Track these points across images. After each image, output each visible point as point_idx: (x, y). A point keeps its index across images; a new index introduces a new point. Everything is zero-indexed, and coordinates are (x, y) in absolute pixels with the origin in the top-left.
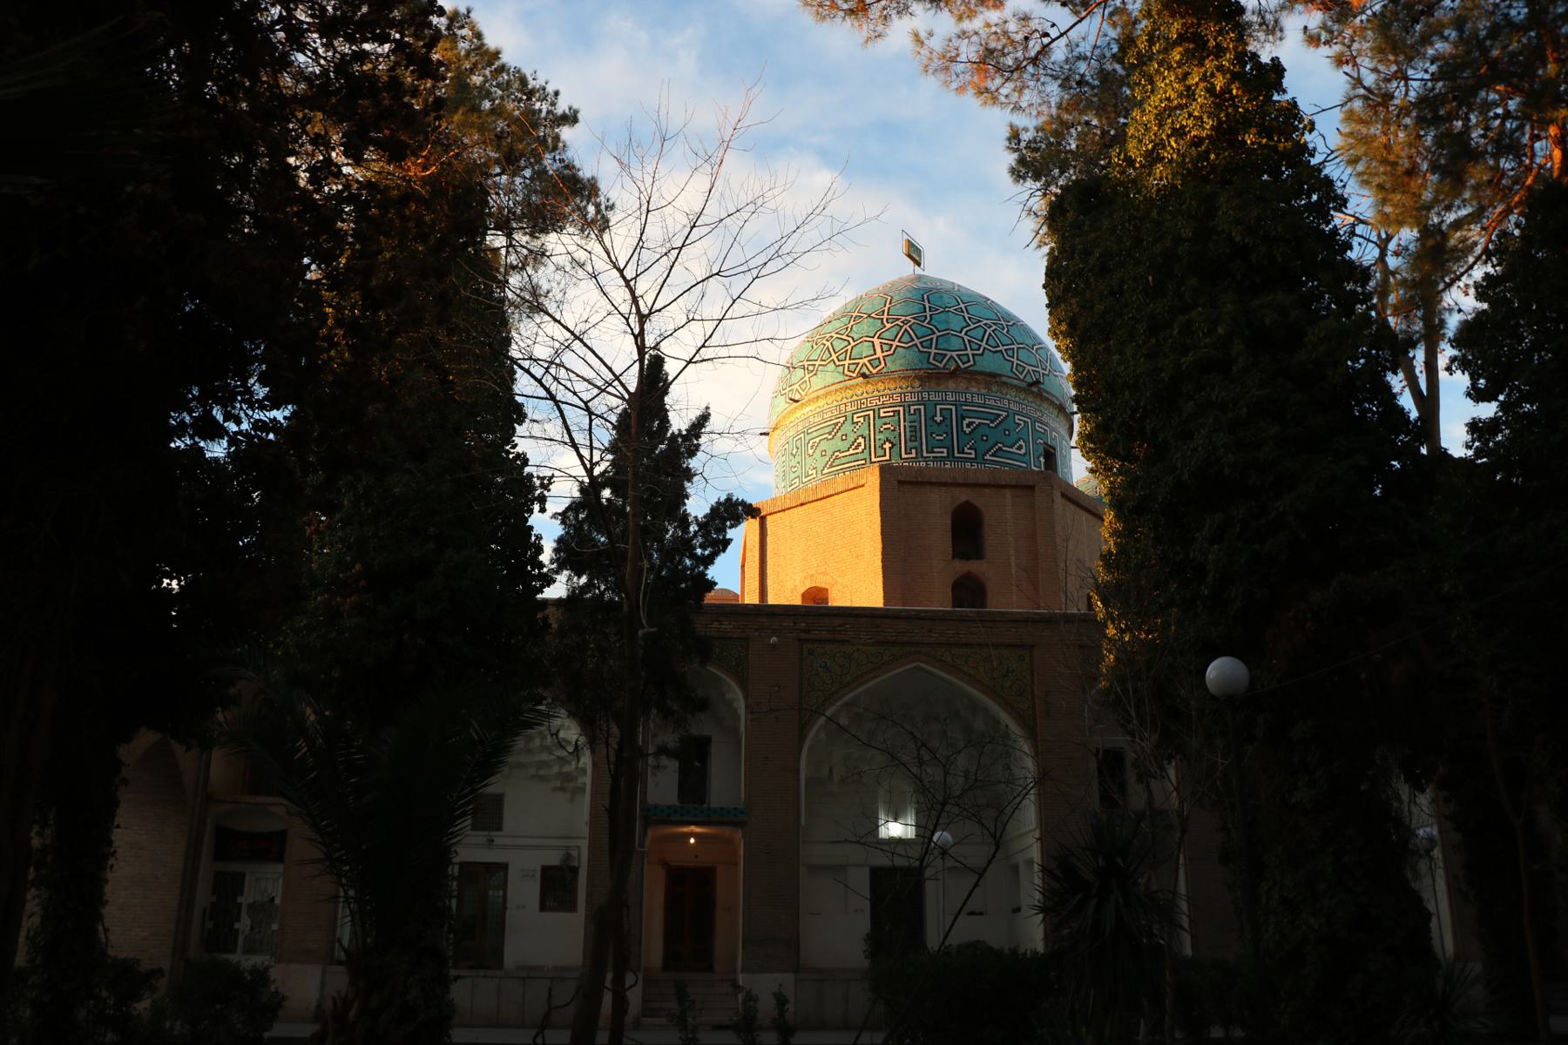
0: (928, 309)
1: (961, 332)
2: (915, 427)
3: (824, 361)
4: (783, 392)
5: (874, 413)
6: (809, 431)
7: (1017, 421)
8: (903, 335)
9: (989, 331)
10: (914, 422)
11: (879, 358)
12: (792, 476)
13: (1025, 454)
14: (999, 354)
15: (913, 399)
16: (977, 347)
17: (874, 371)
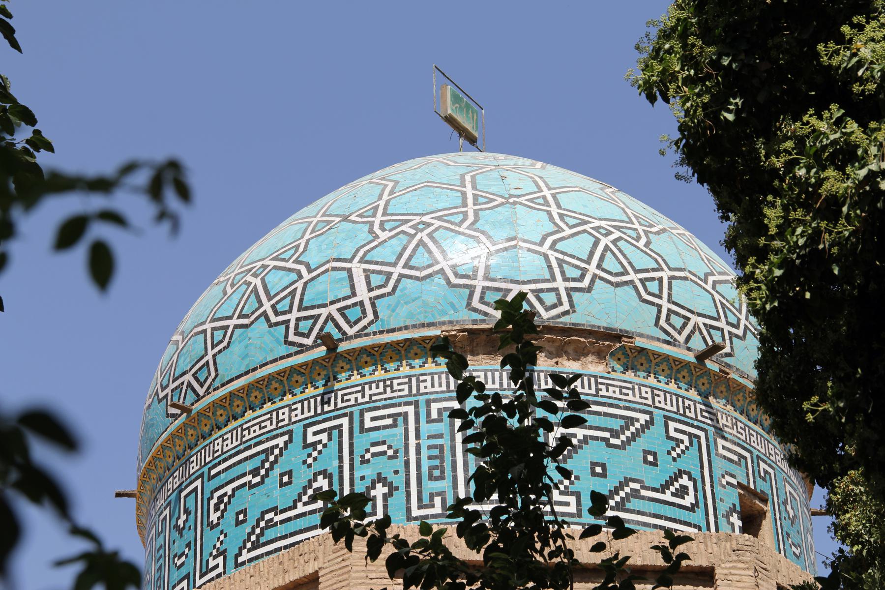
0: (470, 201)
1: (541, 244)
2: (441, 448)
3: (246, 316)
4: (161, 395)
5: (351, 422)
6: (213, 472)
7: (672, 433)
8: (414, 251)
9: (604, 241)
10: (441, 436)
11: (361, 303)
12: (176, 575)
13: (693, 508)
14: (629, 289)
15: (437, 389)
16: (577, 273)
17: (351, 332)
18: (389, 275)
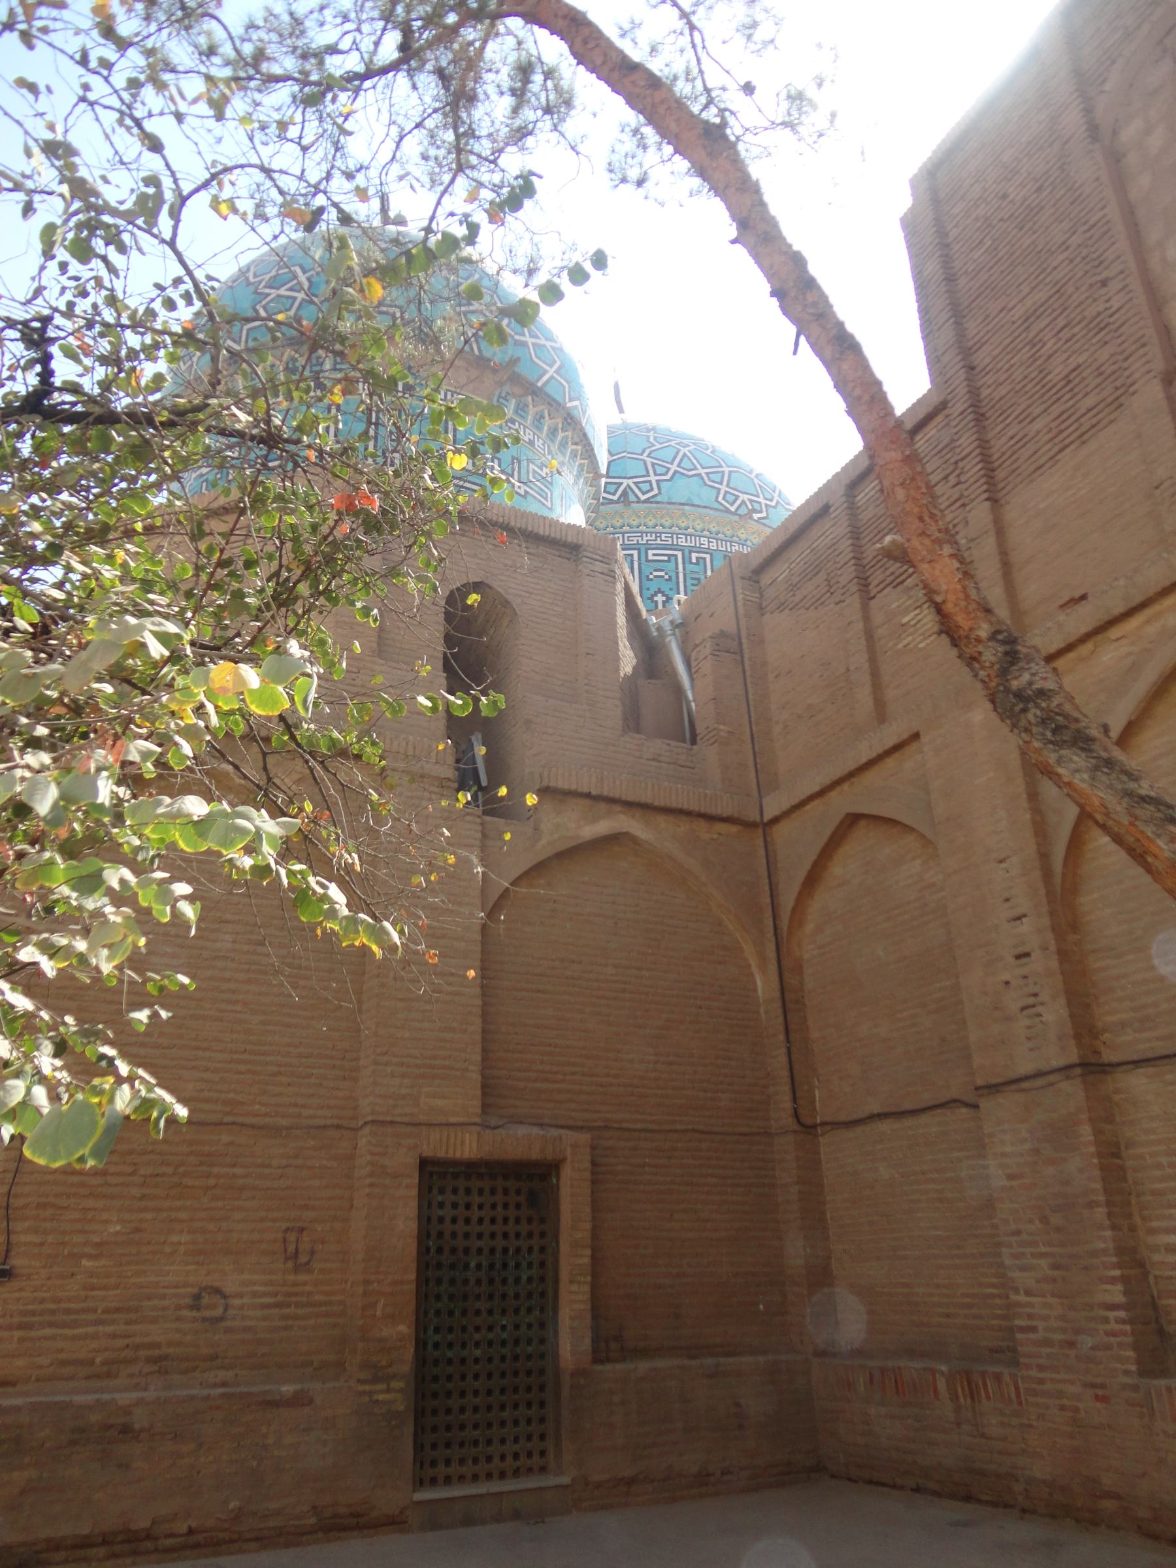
18: (668, 469)
